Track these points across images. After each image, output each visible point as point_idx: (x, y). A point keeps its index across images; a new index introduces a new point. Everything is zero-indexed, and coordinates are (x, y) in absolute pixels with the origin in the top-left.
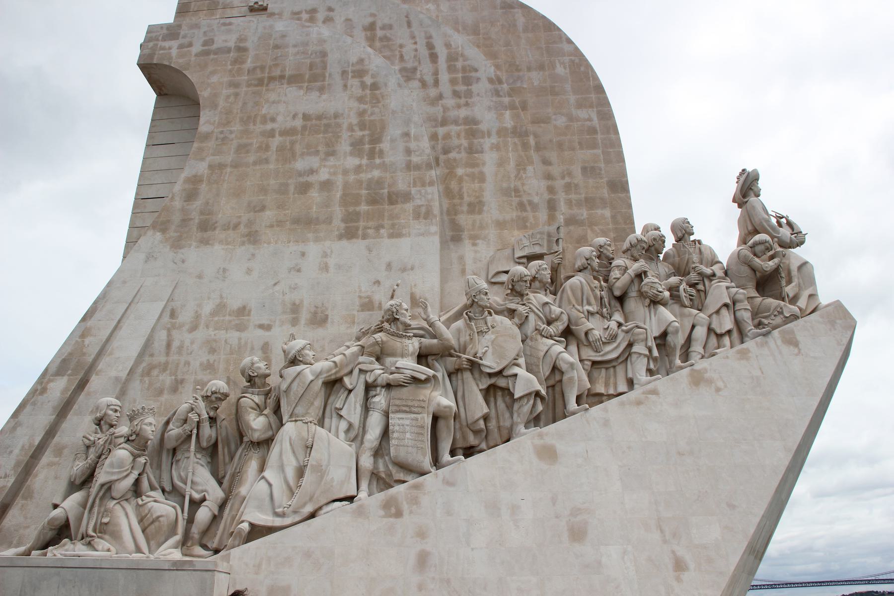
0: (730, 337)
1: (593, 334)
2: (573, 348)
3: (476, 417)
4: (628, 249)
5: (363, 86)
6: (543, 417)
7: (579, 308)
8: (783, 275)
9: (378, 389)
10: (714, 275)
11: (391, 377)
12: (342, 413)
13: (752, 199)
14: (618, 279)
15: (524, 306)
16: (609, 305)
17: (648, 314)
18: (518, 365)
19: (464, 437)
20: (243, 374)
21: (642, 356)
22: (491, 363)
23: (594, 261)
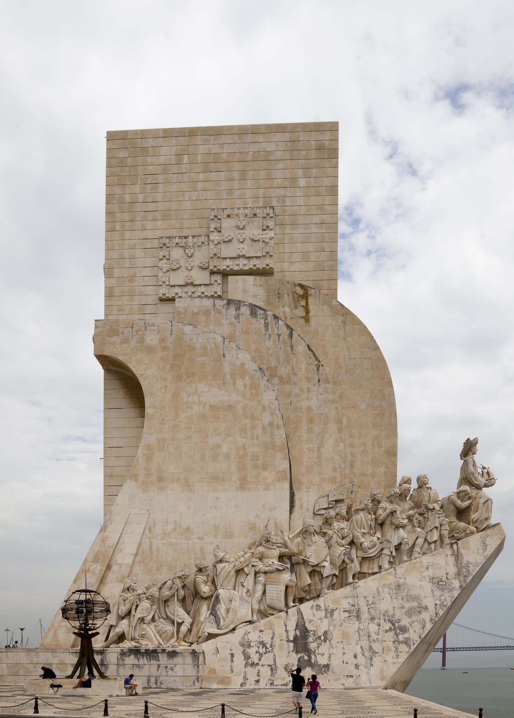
2: (354, 551)
3: (305, 585)
5: (245, 386)
6: (336, 584)
9: (261, 574)
11: (267, 568)
12: (244, 584)
13: (469, 458)
14: (381, 515)
15: (331, 531)
17: (394, 534)
18: (326, 561)
19: (299, 593)
20: (196, 566)
22: (313, 560)
23: (369, 505)
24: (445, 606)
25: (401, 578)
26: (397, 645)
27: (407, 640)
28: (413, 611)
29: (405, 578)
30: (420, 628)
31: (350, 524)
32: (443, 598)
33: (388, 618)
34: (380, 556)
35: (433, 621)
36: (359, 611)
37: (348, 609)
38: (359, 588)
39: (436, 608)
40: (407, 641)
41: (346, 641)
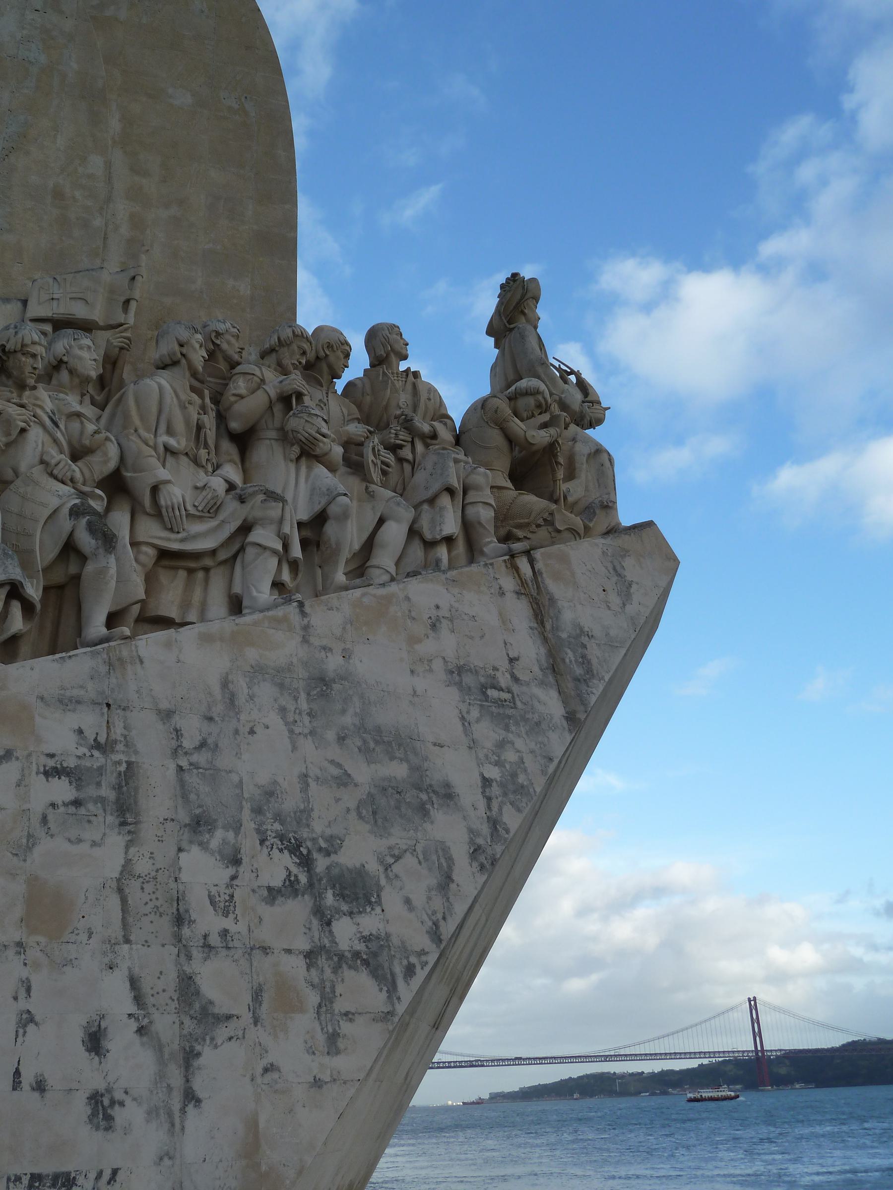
0: (449, 551)
1: (169, 492)
4: (272, 350)
7: (149, 436)
8: (561, 460)
10: (434, 436)
14: (241, 397)
16: (216, 447)
21: (267, 553)
23: (194, 349)
24: (521, 790)
25: (330, 648)
26: (328, 972)
27: (374, 946)
28: (392, 803)
29: (347, 655)
30: (430, 890)
31: (113, 416)
32: (510, 756)
33: (277, 826)
34: (235, 557)
35: (482, 858)
36: (130, 771)
37: (71, 763)
38: (138, 666)
39: (489, 799)
40: (375, 955)
41: (41, 939)
